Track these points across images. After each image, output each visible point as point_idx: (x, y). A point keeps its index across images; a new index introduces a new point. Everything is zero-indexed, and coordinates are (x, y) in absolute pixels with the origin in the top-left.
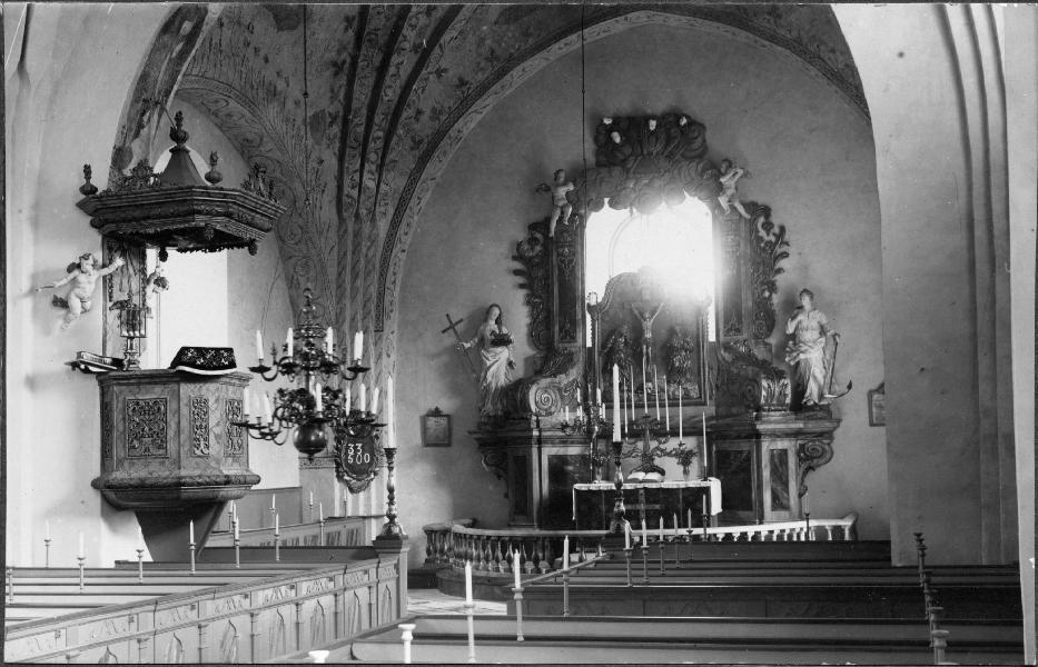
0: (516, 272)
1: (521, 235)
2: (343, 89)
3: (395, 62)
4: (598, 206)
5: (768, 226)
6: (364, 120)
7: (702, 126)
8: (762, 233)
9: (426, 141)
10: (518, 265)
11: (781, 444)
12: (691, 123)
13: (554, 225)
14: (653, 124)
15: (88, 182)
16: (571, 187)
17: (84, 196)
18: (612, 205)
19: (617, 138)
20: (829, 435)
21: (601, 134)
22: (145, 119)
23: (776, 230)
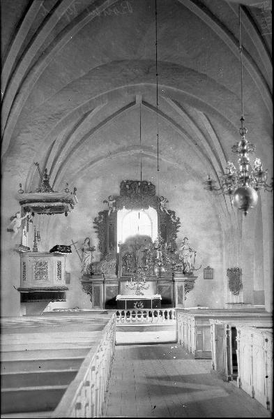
0: (94, 227)
1: (98, 216)
4: (122, 208)
5: (174, 217)
7: (155, 186)
8: (173, 220)
12: (151, 184)
13: (109, 213)
16: (114, 201)
18: (126, 208)
19: (127, 186)
20: (193, 281)
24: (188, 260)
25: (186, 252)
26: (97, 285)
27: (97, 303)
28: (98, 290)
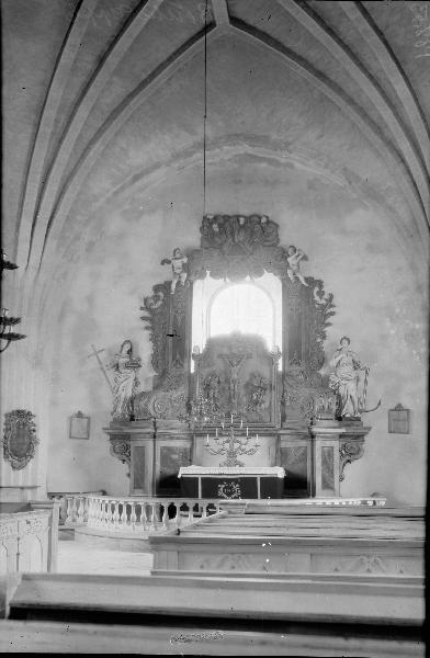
0: (143, 318)
1: (150, 293)
4: (202, 276)
5: (321, 294)
7: (277, 226)
8: (317, 298)
10: (146, 314)
11: (328, 443)
12: (268, 222)
13: (174, 286)
14: (242, 221)
21: (207, 223)
23: (326, 296)
24: (349, 389)
25: (346, 370)
26: (140, 444)
27: (138, 484)
28: (141, 451)
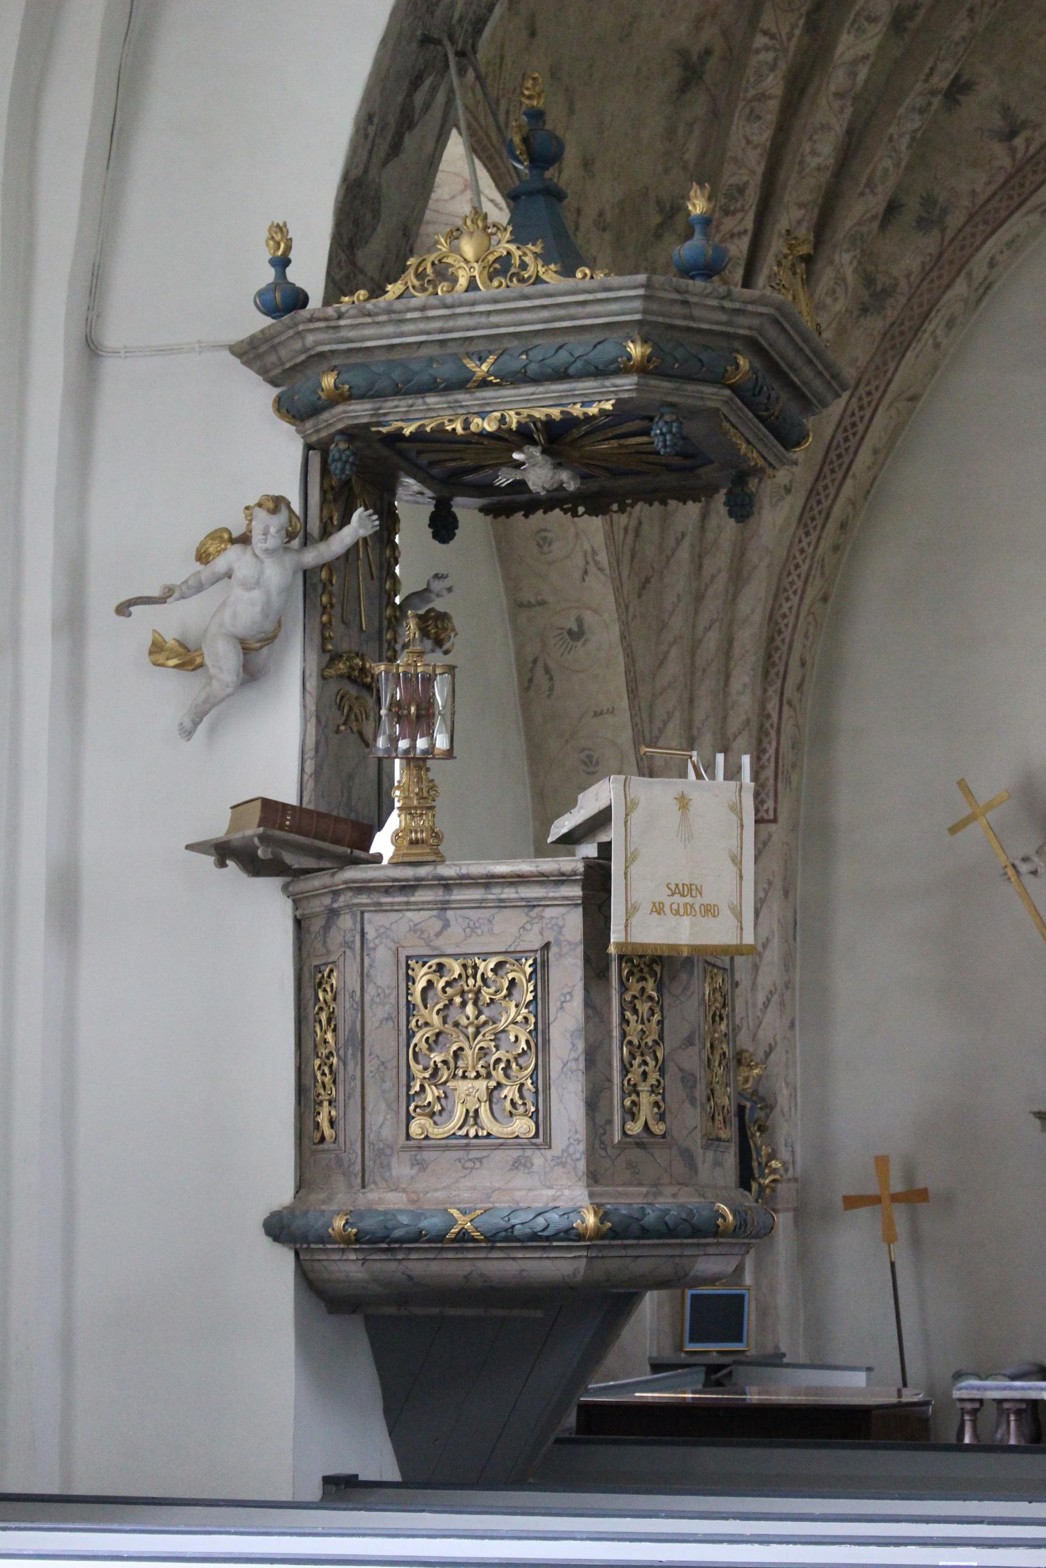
2: (697, 132)
3: (848, 57)
6: (749, 224)
9: (903, 283)
15: (281, 274)
17: (268, 321)
22: (419, 99)
